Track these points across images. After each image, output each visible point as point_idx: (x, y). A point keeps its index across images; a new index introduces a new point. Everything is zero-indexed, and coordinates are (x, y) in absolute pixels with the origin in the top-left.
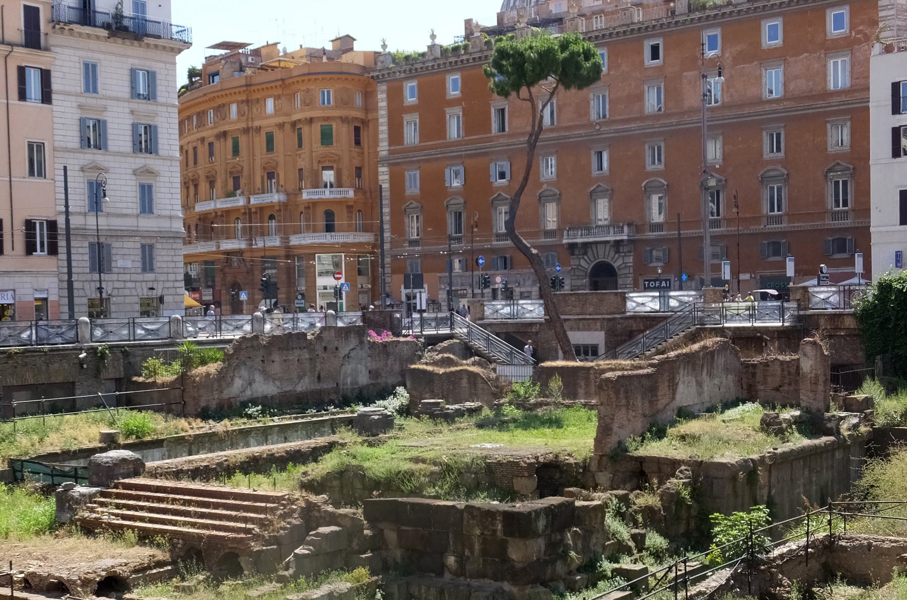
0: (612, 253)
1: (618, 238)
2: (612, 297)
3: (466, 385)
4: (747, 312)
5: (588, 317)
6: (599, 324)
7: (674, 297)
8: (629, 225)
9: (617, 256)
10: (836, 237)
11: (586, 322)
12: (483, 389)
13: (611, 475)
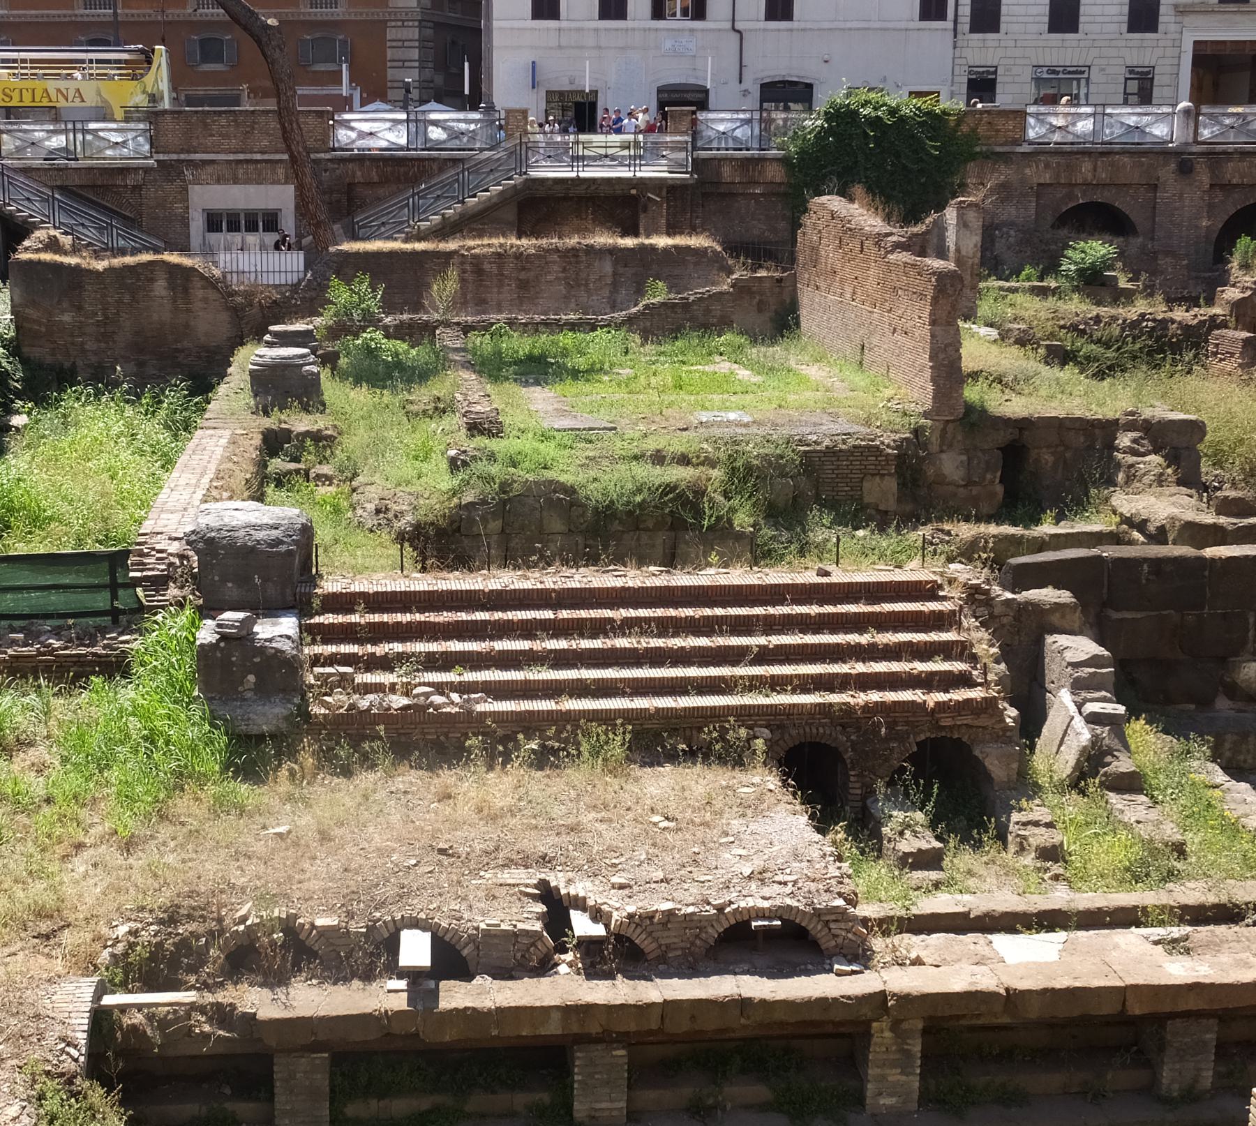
2: (310, 120)
3: (164, 293)
4: (626, 152)
5: (258, 157)
7: (435, 123)
10: (318, 35)
11: (251, 167)
12: (205, 300)
13: (964, 458)
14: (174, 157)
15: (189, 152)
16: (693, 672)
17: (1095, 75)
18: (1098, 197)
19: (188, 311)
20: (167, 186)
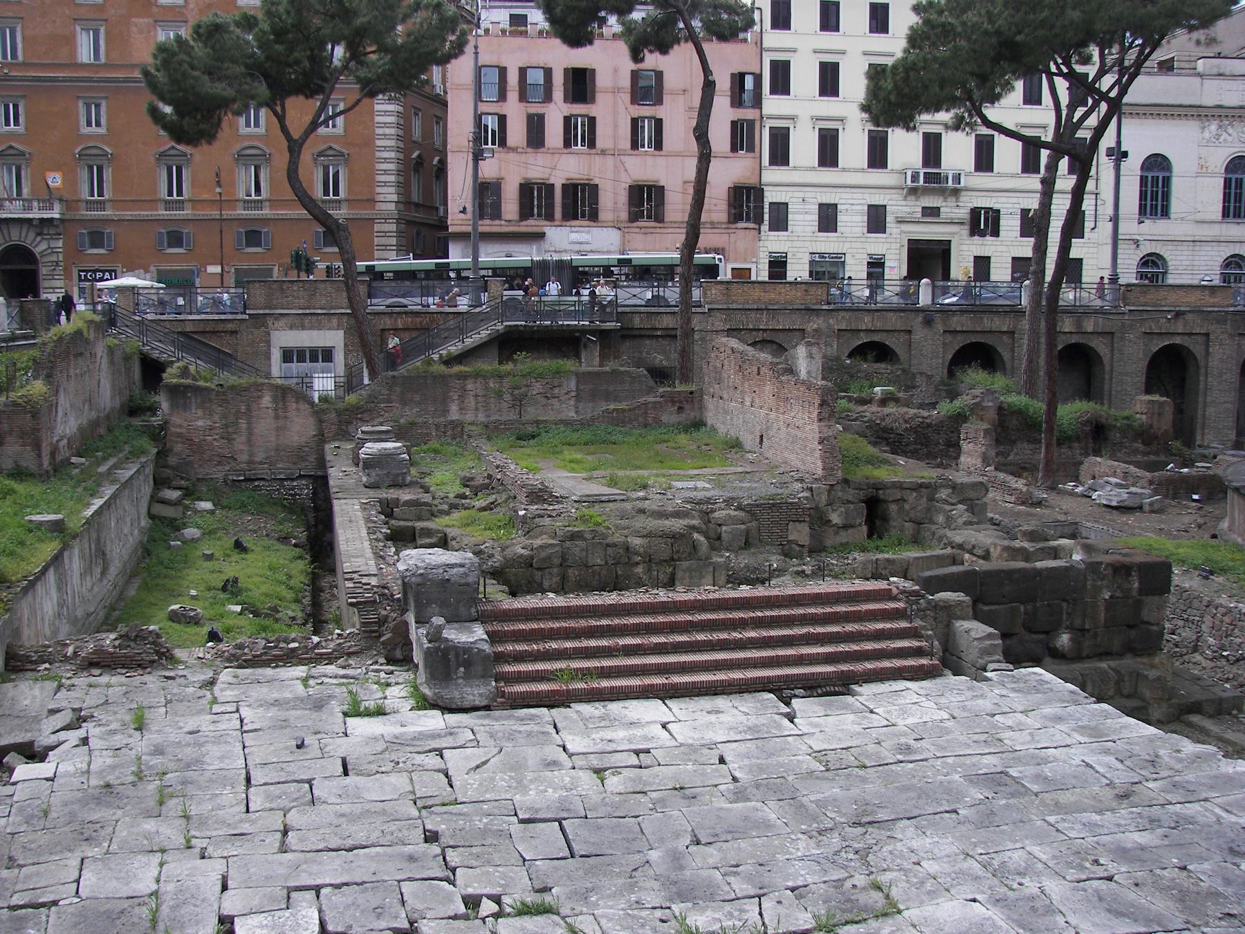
0: (32, 235)
1: (45, 216)
3: (270, 405)
6: (335, 321)
8: (61, 200)
9: (39, 238)
11: (314, 318)
12: (298, 410)
14: (261, 312)
15: (270, 308)
16: (869, 646)
17: (849, 260)
18: (876, 338)
19: (286, 417)
20: (256, 332)
